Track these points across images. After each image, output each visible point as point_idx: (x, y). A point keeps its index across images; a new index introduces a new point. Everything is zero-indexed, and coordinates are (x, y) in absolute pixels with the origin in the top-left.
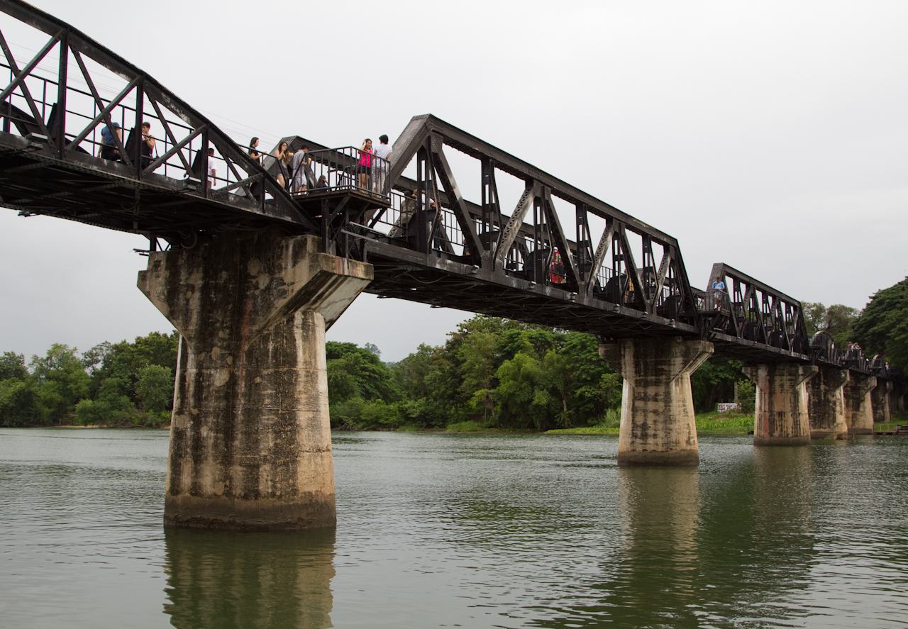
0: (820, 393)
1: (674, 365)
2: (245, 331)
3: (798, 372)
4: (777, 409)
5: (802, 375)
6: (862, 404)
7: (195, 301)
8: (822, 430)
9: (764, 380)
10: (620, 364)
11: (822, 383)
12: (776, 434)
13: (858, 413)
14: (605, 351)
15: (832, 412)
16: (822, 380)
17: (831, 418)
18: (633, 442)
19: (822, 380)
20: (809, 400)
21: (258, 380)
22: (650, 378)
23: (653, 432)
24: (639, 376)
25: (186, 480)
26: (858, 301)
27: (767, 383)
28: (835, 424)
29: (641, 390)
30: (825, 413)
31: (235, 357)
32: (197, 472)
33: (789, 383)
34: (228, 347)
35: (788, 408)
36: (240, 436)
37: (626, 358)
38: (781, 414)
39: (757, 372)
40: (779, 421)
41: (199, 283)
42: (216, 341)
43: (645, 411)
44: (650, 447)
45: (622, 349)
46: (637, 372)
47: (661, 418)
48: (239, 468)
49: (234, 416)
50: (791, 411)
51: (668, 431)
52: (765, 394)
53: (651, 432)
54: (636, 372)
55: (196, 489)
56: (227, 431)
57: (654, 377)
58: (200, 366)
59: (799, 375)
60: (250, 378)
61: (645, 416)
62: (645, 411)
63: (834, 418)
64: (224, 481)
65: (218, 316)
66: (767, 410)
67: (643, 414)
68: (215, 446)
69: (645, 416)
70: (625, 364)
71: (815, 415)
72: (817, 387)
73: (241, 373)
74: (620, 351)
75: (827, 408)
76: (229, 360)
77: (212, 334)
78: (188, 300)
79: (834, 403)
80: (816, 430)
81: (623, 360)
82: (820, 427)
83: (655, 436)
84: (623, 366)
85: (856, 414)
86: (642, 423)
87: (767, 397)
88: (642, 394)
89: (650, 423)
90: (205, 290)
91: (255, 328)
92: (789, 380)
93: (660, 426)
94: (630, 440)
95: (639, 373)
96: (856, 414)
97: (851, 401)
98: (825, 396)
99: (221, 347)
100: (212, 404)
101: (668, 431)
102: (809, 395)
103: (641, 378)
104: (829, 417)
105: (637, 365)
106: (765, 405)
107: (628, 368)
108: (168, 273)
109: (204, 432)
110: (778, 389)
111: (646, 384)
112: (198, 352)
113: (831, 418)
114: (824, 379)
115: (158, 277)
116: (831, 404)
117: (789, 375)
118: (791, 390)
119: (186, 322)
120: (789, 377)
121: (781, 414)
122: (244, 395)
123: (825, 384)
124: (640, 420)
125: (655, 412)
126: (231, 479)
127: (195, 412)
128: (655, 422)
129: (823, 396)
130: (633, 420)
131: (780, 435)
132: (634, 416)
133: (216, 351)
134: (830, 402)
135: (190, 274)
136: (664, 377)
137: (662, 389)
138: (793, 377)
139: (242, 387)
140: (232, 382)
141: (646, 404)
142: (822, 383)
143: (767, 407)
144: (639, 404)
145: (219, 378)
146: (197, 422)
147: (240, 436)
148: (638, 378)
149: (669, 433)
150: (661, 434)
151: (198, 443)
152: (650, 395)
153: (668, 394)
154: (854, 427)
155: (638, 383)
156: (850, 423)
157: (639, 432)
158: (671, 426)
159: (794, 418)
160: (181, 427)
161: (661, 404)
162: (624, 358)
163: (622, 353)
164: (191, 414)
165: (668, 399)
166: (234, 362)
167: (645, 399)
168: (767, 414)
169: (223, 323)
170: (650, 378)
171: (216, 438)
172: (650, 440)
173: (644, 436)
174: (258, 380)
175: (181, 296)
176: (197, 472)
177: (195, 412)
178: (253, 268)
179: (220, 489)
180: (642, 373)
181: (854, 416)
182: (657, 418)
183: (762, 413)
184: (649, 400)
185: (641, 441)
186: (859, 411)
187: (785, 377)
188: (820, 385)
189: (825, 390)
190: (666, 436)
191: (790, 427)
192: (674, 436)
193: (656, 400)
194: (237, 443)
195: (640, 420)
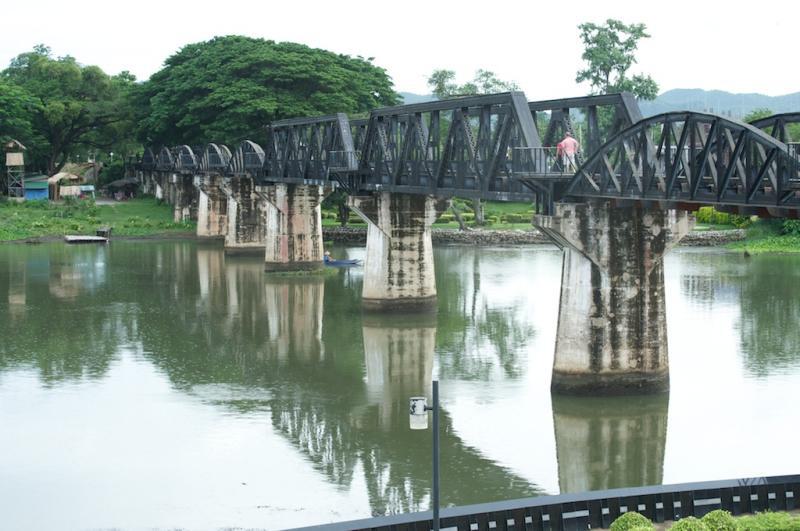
2: (648, 262)
4: (296, 231)
7: (604, 240)
8: (253, 244)
10: (376, 216)
15: (262, 224)
17: (262, 231)
18: (390, 289)
20: (238, 210)
21: (656, 294)
22: (405, 229)
25: (606, 359)
26: (145, 67)
27: (286, 203)
29: (396, 240)
30: (255, 225)
31: (642, 281)
32: (615, 354)
33: (309, 204)
34: (635, 273)
35: (308, 230)
36: (648, 330)
37: (383, 210)
38: (301, 237)
39: (274, 191)
41: (606, 229)
42: (625, 268)
44: (406, 294)
46: (393, 222)
48: (648, 350)
49: (643, 317)
53: (406, 278)
55: (615, 364)
56: (637, 325)
58: (613, 285)
60: (652, 291)
61: (401, 264)
64: (637, 358)
65: (623, 252)
66: (286, 232)
68: (629, 336)
73: (647, 289)
74: (376, 203)
75: (258, 220)
76: (637, 281)
77: (620, 265)
78: (598, 241)
82: (251, 241)
86: (398, 270)
87: (286, 217)
89: (406, 270)
90: (611, 233)
91: (654, 261)
93: (416, 273)
94: (387, 287)
97: (218, 203)
98: (255, 206)
99: (630, 273)
100: (625, 310)
102: (238, 205)
104: (260, 229)
105: (393, 217)
107: (384, 219)
108: (578, 220)
109: (620, 328)
110: (297, 210)
111: (402, 235)
112: (612, 275)
113: (262, 231)
115: (570, 222)
117: (310, 195)
118: (310, 211)
119: (599, 256)
120: (309, 198)
121: (301, 237)
122: (649, 304)
124: (396, 268)
126: (642, 357)
127: (612, 315)
128: (411, 269)
131: (301, 258)
133: (626, 276)
134: (260, 212)
135: (598, 222)
136: (419, 228)
137: (416, 240)
138: (313, 198)
139: (647, 300)
140: (641, 294)
144: (395, 253)
145: (630, 293)
146: (614, 322)
147: (648, 330)
150: (416, 280)
151: (615, 336)
155: (394, 234)
156: (217, 229)
157: (395, 279)
160: (600, 326)
164: (608, 317)
166: (641, 283)
167: (401, 248)
168: (286, 237)
169: (629, 257)
170: (405, 229)
171: (630, 332)
172: (406, 286)
173: (401, 283)
174: (656, 294)
175: (592, 237)
176: (615, 354)
177: (612, 315)
178: (648, 221)
179: (634, 363)
185: (398, 287)
187: (304, 198)
193: (412, 250)
194: (646, 334)
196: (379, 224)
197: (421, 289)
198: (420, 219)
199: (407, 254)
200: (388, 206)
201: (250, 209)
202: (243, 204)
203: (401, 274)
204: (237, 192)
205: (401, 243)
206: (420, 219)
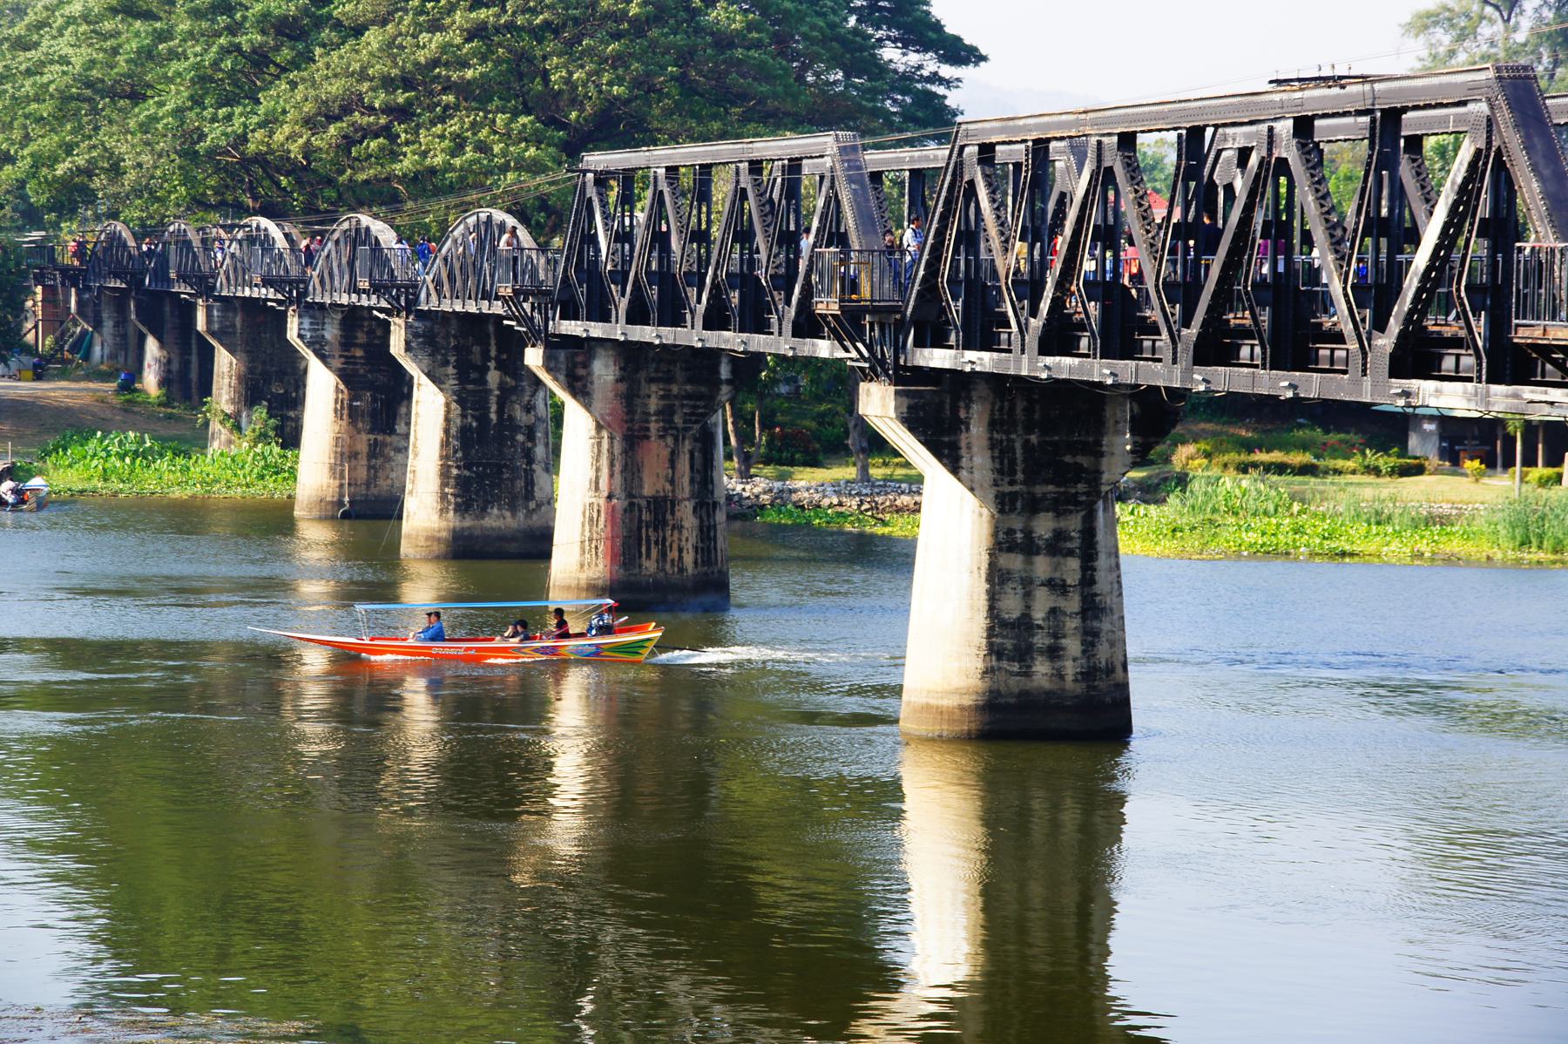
0: (487, 402)
1: (1113, 454)
3: (718, 372)
5: (728, 382)
6: (403, 410)
9: (611, 395)
10: (954, 447)
11: (492, 364)
12: (650, 566)
13: (388, 439)
14: (909, 407)
15: (521, 463)
16: (493, 353)
19: (493, 353)
22: (1039, 490)
23: (1048, 641)
24: (1012, 483)
28: (532, 505)
29: (1017, 523)
30: (499, 469)
35: (685, 486)
37: (974, 430)
38: (662, 507)
39: (586, 365)
40: (656, 530)
43: (1027, 583)
45: (962, 404)
47: (1073, 604)
50: (693, 496)
51: (1090, 639)
52: (611, 438)
53: (1041, 640)
54: (1000, 472)
57: (1051, 488)
59: (720, 382)
61: (1028, 595)
62: (1027, 583)
63: (530, 483)
66: (618, 492)
67: (1020, 590)
69: (1028, 595)
70: (969, 447)
71: (467, 473)
72: (473, 375)
74: (955, 410)
79: (530, 433)
80: (468, 523)
81: (963, 436)
83: (1054, 653)
84: (963, 452)
85: (384, 444)
88: (1019, 535)
89: (1039, 615)
92: (689, 397)
93: (1072, 624)
95: (1013, 472)
96: (384, 444)
98: (500, 412)
101: (1090, 638)
102: (447, 405)
103: (1017, 488)
104: (512, 480)
106: (611, 476)
107: (978, 460)
111: (1034, 507)
113: (520, 484)
114: (499, 351)
116: (520, 438)
117: (690, 381)
121: (662, 507)
123: (501, 366)
124: (1012, 606)
125: (1057, 586)
129: (494, 408)
130: (991, 608)
132: (993, 598)
134: (515, 428)
136: (1081, 487)
137: (1074, 523)
141: (1031, 563)
142: (492, 364)
143: (618, 478)
144: (1014, 562)
148: (1007, 489)
149: (1093, 644)
150: (1073, 645)
152: (1040, 537)
153: (1089, 533)
154: (374, 491)
156: (362, 473)
158: (1096, 624)
159: (701, 520)
161: (1074, 564)
162: (968, 429)
163: (962, 415)
165: (1088, 553)
167: (1029, 548)
170: (1039, 490)
172: (1041, 668)
173: (1023, 654)
180: (1020, 476)
181: (375, 451)
182: (1061, 603)
183: (602, 502)
184: (1038, 554)
185: (1016, 667)
186: (392, 431)
188: (488, 369)
189: (502, 386)
190: (1084, 652)
191: (690, 546)
192: (1103, 653)
195: (1012, 606)
196: (964, 473)
197: (1089, 674)
198: (1084, 461)
199: (1042, 566)
200: (986, 418)
201: (483, 419)
202: (461, 402)
203: (1024, 624)
204: (446, 363)
205: (1028, 533)
206: (1084, 461)
